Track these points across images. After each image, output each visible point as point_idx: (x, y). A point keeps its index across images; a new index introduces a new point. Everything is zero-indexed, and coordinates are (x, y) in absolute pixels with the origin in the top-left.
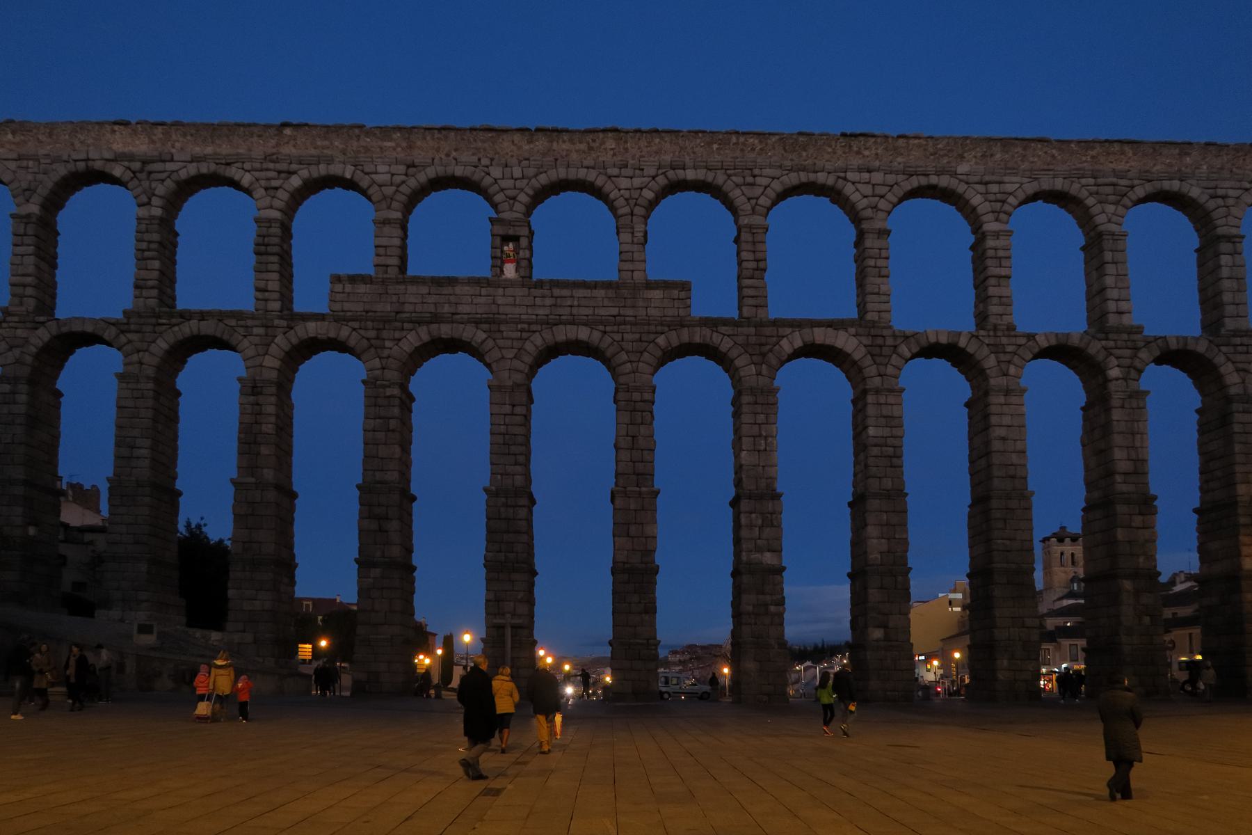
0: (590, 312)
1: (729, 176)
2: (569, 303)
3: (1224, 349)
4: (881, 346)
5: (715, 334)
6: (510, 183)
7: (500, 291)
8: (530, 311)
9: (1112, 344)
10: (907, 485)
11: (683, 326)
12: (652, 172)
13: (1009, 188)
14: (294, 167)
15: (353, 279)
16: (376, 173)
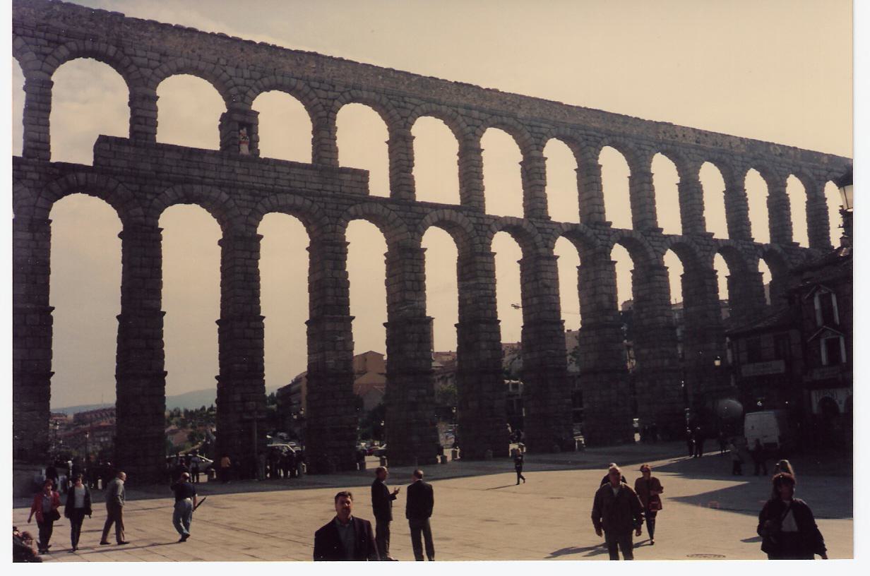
0: (303, 185)
1: (390, 99)
2: (288, 177)
3: (648, 238)
4: (481, 225)
5: (385, 209)
6: (240, 81)
7: (237, 164)
8: (260, 181)
9: (597, 232)
10: (499, 314)
11: (364, 201)
12: (342, 89)
13: (543, 130)
14: (63, 39)
15: (119, 141)
16: (135, 56)
